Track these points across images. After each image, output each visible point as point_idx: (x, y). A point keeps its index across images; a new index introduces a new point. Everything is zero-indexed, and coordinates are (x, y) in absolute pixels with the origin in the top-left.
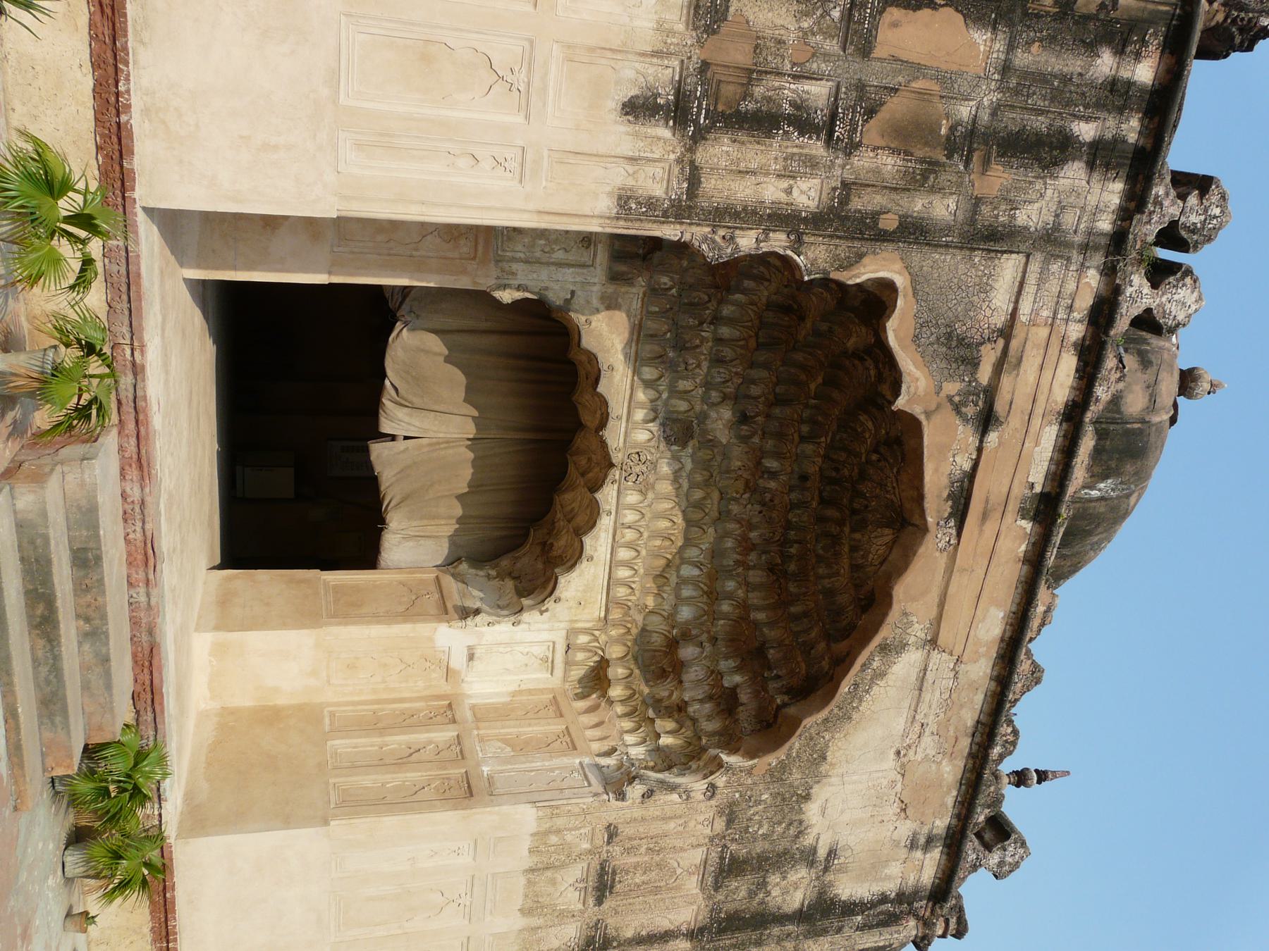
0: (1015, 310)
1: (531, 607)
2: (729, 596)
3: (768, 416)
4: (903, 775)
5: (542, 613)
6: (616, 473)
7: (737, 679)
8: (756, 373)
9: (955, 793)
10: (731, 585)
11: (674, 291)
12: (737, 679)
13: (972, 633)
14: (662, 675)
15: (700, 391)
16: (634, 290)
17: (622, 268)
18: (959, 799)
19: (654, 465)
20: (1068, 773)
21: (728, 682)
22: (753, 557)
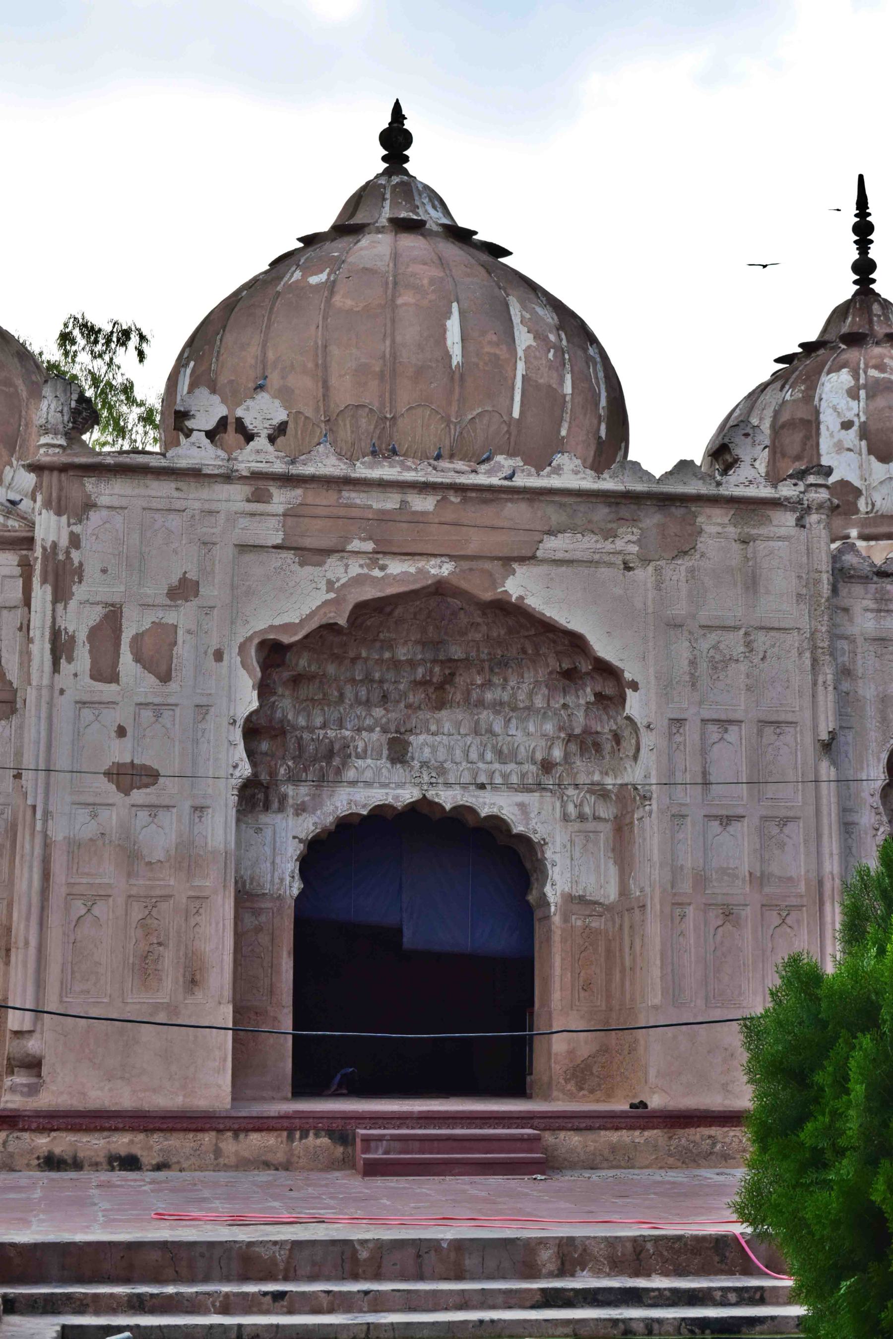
0: (276, 547)
1: (543, 852)
2: (531, 694)
3: (381, 681)
4: (650, 561)
5: (546, 844)
6: (431, 794)
7: (588, 690)
8: (349, 691)
9: (673, 509)
10: (522, 696)
11: (290, 763)
12: (588, 690)
13: (523, 527)
14: (597, 747)
15: (364, 734)
16: (291, 793)
17: (276, 805)
18: (678, 504)
19: (424, 764)
20: (861, 177)
21: (592, 699)
22: (495, 680)
